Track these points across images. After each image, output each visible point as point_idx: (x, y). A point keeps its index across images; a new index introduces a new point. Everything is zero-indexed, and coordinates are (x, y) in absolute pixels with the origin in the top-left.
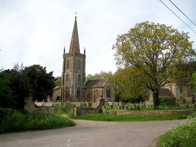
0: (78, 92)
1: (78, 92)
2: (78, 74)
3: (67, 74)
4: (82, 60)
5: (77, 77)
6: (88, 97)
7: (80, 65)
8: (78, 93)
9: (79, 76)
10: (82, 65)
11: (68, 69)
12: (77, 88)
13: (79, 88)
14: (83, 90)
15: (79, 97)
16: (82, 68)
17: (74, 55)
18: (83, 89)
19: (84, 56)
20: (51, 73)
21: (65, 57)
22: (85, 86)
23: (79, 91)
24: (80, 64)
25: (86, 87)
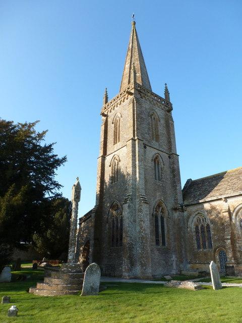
0: (157, 221)
1: (157, 221)
2: (151, 153)
3: (114, 158)
4: (160, 112)
5: (151, 164)
6: (198, 240)
7: (156, 128)
8: (157, 227)
9: (156, 160)
10: (162, 130)
11: (115, 143)
12: (154, 203)
13: (159, 206)
14: (176, 215)
15: (164, 243)
16: (163, 139)
17: (133, 91)
18: (175, 209)
19: (168, 107)
20: (53, 149)
21: (106, 113)
22: (180, 197)
23: (162, 218)
24: (156, 125)
25: (186, 203)
